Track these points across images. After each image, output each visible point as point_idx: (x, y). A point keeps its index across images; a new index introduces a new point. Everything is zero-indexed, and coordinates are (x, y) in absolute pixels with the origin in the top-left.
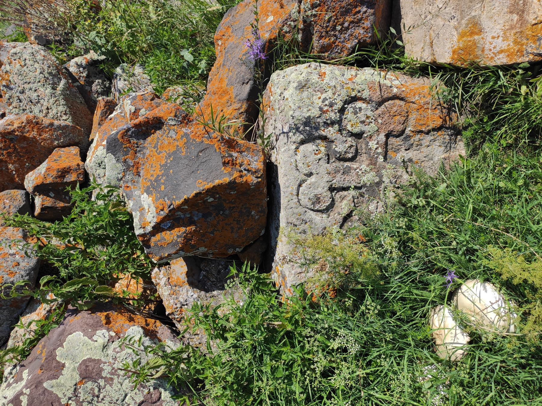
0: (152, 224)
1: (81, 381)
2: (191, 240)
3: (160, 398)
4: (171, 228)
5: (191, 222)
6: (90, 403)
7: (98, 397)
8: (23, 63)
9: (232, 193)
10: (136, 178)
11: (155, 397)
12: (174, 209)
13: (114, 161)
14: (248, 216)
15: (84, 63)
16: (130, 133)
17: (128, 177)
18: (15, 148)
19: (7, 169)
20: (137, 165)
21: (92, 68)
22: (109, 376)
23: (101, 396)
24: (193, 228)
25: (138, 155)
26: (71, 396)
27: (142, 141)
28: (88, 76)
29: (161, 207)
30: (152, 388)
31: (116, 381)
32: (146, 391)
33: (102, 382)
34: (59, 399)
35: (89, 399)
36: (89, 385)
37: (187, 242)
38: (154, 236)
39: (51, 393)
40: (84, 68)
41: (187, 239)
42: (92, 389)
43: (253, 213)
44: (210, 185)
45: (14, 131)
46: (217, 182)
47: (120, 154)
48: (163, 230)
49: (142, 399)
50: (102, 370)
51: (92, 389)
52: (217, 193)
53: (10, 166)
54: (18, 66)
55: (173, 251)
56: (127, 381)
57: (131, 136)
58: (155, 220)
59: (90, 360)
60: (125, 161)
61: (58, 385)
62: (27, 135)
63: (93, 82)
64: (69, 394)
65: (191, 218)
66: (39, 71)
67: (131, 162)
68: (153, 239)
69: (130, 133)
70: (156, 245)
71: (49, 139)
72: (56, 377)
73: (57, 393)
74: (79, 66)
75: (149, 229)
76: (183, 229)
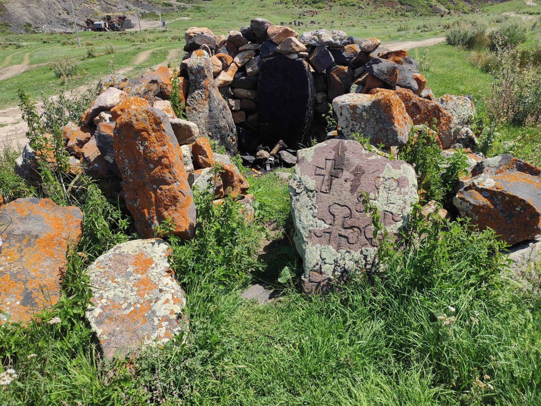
0: (483, 187)
1: (395, 180)
2: (483, 209)
3: (397, 221)
4: (484, 197)
5: (495, 205)
6: (384, 188)
7: (389, 190)
8: (464, 105)
9: (528, 218)
10: (494, 173)
11: (396, 219)
12: (503, 193)
13: (498, 160)
14: (509, 234)
15: (471, 135)
16: (518, 163)
17: (493, 170)
18: (430, 115)
19: (416, 115)
20: (501, 171)
21: (468, 140)
22: (402, 192)
23: (390, 192)
24: (492, 207)
25: (507, 170)
26: (386, 177)
27: (516, 169)
28: (462, 139)
29: (499, 187)
30: (402, 215)
31: (401, 196)
32: (400, 213)
33: (398, 189)
34: (382, 173)
35: (386, 187)
36: (395, 184)
37: (481, 207)
38: (476, 190)
39: (384, 168)
40: (466, 136)
41: (483, 207)
42: (393, 186)
43: (512, 236)
44: (532, 205)
45: (441, 112)
46: (535, 207)
47: (504, 162)
48: (481, 194)
49: (394, 212)
50: (405, 188)
51: (393, 186)
52: (524, 211)
53: (418, 116)
54: (461, 103)
55: (472, 202)
56: (402, 202)
57: (517, 164)
58: (488, 188)
59: (408, 180)
60: (501, 165)
61: (390, 170)
62: (441, 118)
63: (459, 143)
64: (387, 177)
65: (497, 204)
66: (464, 113)
67: (501, 168)
68: (473, 191)
69: (518, 163)
70: (470, 193)
71: (443, 130)
72: (394, 167)
73: (385, 171)
74: (467, 132)
75: (480, 187)
76: (489, 203)
